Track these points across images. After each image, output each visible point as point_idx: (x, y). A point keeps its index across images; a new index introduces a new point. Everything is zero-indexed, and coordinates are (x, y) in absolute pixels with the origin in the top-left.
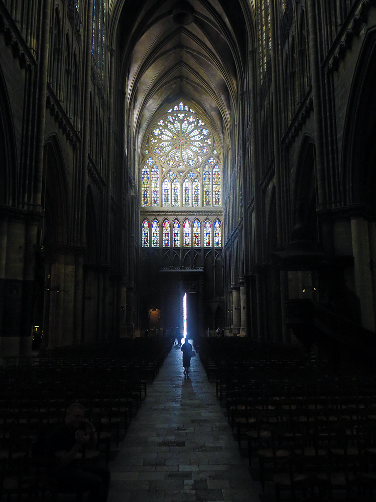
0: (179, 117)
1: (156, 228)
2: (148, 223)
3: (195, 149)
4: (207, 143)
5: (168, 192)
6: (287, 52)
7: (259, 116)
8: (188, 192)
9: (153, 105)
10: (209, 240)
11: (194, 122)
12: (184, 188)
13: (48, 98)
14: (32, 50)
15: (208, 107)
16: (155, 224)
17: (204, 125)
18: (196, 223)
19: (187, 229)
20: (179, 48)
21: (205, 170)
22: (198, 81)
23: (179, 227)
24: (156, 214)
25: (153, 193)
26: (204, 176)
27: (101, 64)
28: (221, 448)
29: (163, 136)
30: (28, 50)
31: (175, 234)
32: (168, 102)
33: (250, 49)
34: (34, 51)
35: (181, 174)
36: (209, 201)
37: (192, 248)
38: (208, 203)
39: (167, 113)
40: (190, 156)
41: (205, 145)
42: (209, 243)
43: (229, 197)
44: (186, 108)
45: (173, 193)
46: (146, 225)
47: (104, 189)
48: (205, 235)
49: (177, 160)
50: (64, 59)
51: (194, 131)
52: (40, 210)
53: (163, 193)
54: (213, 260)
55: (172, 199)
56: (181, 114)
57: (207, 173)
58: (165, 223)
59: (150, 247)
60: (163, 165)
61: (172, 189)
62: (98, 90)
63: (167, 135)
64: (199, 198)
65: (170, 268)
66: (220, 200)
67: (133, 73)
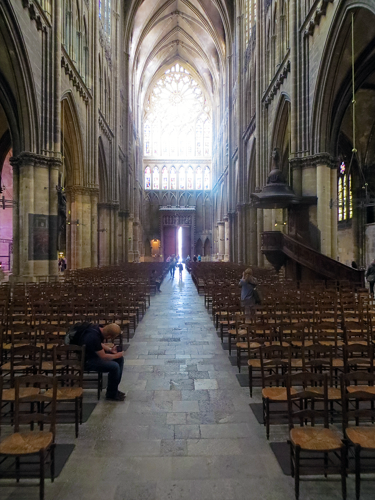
6: (270, 18)
7: (244, 77)
9: (153, 65)
13: (63, 58)
14: (47, 13)
15: (201, 68)
16: (156, 170)
20: (176, 14)
22: (192, 45)
24: (156, 162)
27: (108, 28)
28: (208, 342)
30: (42, 13)
32: (166, 63)
33: (237, 15)
34: (48, 13)
43: (217, 148)
44: (182, 69)
47: (112, 140)
50: (75, 22)
52: (59, 156)
56: (177, 74)
59: (152, 190)
62: (105, 52)
65: (168, 207)
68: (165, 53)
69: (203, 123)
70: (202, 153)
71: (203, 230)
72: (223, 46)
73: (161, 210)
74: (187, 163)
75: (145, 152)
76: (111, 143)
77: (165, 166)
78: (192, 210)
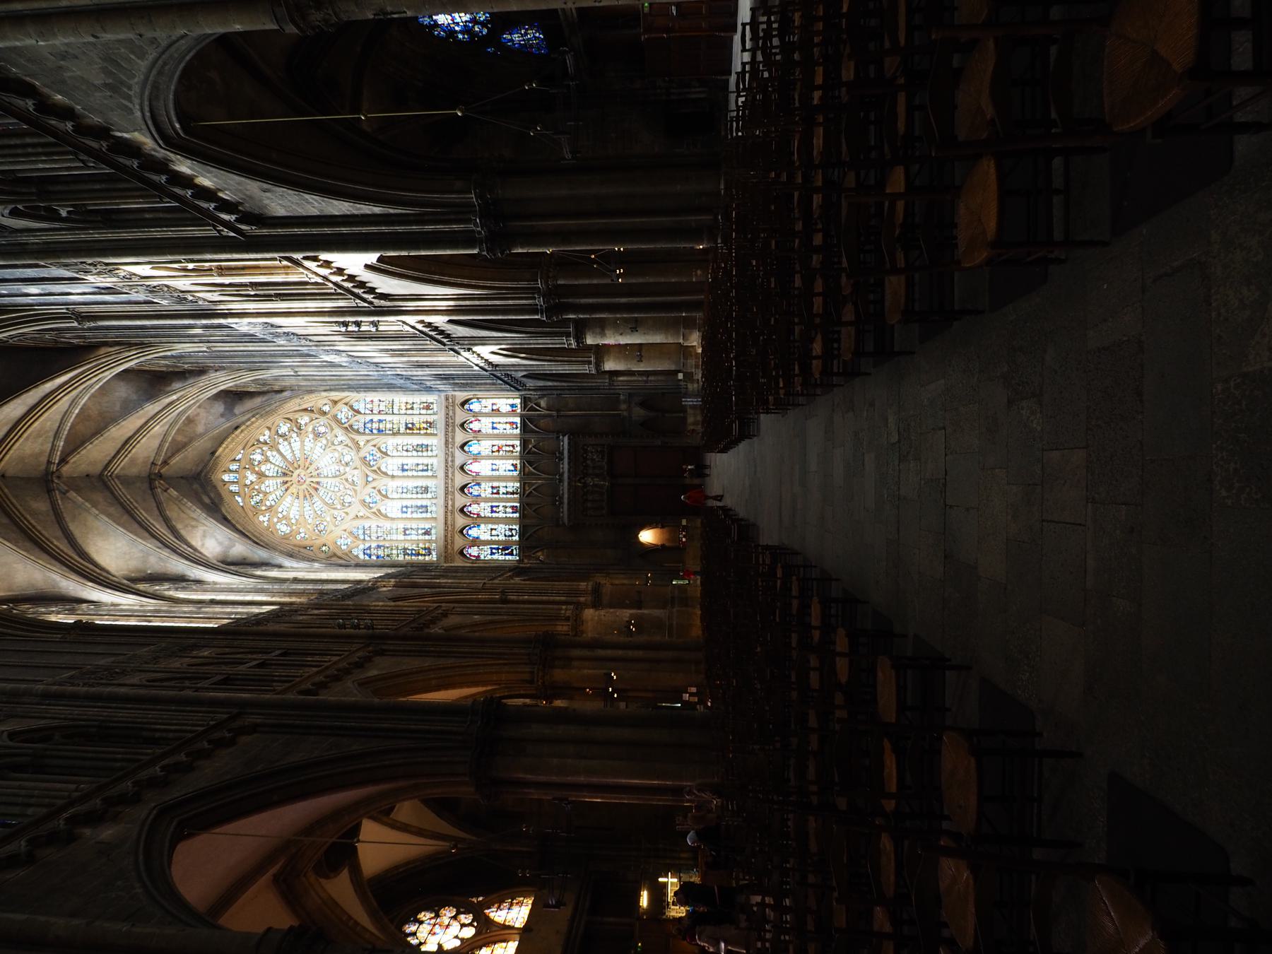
0: (252, 483)
1: (482, 532)
2: (470, 547)
3: (318, 450)
4: (306, 424)
5: (407, 507)
10: (506, 423)
11: (263, 450)
12: (400, 473)
16: (474, 532)
17: (269, 429)
19: (483, 468)
21: (361, 430)
23: (479, 484)
24: (451, 532)
25: (409, 538)
26: (375, 431)
29: (292, 516)
31: (493, 493)
35: (370, 479)
36: (427, 422)
37: (521, 458)
38: (430, 423)
40: (334, 459)
41: (310, 429)
42: (512, 423)
43: (408, 378)
44: (234, 467)
45: (409, 496)
46: (474, 551)
48: (496, 431)
49: (342, 486)
51: (282, 451)
53: (409, 515)
54: (545, 416)
56: (246, 477)
57: (369, 425)
58: (470, 512)
59: (520, 543)
60: (352, 515)
61: (400, 499)
63: (291, 507)
64: (420, 443)
65: (562, 503)
67: (83, 590)
68: (183, 508)
69: (359, 416)
70: (430, 419)
71: (619, 415)
72: (103, 350)
73: (569, 521)
74: (453, 456)
75: (427, 558)
76: (254, 728)
77: (462, 510)
78: (569, 443)
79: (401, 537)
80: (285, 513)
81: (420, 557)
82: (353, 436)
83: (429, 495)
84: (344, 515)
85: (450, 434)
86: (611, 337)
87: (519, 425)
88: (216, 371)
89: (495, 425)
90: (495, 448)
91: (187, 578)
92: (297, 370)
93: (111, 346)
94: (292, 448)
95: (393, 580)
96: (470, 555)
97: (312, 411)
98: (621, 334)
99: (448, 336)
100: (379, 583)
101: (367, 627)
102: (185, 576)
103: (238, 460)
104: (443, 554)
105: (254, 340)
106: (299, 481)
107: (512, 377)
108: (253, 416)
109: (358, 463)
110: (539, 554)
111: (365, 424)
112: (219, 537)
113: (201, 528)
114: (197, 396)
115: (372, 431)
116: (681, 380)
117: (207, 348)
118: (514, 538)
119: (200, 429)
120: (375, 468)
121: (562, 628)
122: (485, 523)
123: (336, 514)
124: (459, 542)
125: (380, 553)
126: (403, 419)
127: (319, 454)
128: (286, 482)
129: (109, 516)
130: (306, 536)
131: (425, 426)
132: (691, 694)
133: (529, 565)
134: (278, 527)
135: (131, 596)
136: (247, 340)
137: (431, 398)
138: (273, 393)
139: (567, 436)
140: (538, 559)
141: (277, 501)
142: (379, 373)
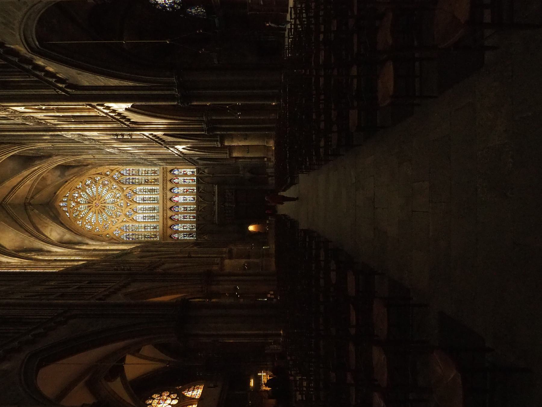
2: (174, 234)
4: (99, 180)
5: (145, 217)
8: (146, 198)
10: (190, 179)
12: (142, 202)
16: (176, 227)
17: (82, 182)
18: (175, 191)
19: (180, 199)
23: (178, 206)
24: (165, 227)
29: (93, 221)
31: (184, 210)
35: (128, 204)
36: (154, 179)
37: (197, 195)
38: (156, 179)
39: (69, 217)
40: (112, 196)
41: (101, 183)
43: (145, 160)
45: (147, 212)
46: (176, 236)
51: (88, 192)
53: (146, 221)
54: (207, 177)
55: (152, 213)
56: (71, 204)
57: (128, 181)
59: (196, 232)
60: (120, 221)
61: (143, 213)
63: (92, 217)
64: (151, 188)
66: (153, 169)
69: (123, 177)
70: (156, 177)
74: (166, 194)
77: (170, 218)
78: (218, 188)
79: (143, 230)
80: (89, 220)
81: (152, 239)
82: (121, 186)
83: (156, 211)
84: (117, 221)
85: (165, 185)
86: (235, 142)
87: (196, 181)
88: (56, 156)
89: (185, 180)
90: (185, 191)
91: (43, 250)
92: (94, 156)
93: (5, 144)
94: (92, 191)
95: (140, 249)
96: (174, 237)
97: (101, 174)
98: (240, 141)
99: (164, 141)
100: (133, 251)
101: (128, 270)
102: (43, 249)
103: (67, 196)
104: (162, 237)
105: (74, 142)
106: (96, 206)
107: (192, 159)
108: (74, 177)
109: (123, 197)
110: (205, 236)
111: (126, 180)
112: (58, 231)
113: (50, 228)
114: (47, 167)
115: (129, 183)
116: (266, 161)
117: (52, 145)
118: (194, 230)
119: (49, 182)
120: (131, 199)
121: (215, 268)
122: (181, 223)
123: (113, 220)
124: (169, 232)
125: (134, 237)
126: (144, 178)
127: (105, 194)
128: (90, 206)
129: (6, 222)
130: (99, 230)
131: (153, 181)
132: (271, 295)
133: (200, 241)
134: (86, 226)
135: (16, 259)
136: (71, 142)
137: (156, 169)
138: (83, 166)
139: (217, 185)
140: (204, 238)
141: (85, 214)
142: (133, 157)
